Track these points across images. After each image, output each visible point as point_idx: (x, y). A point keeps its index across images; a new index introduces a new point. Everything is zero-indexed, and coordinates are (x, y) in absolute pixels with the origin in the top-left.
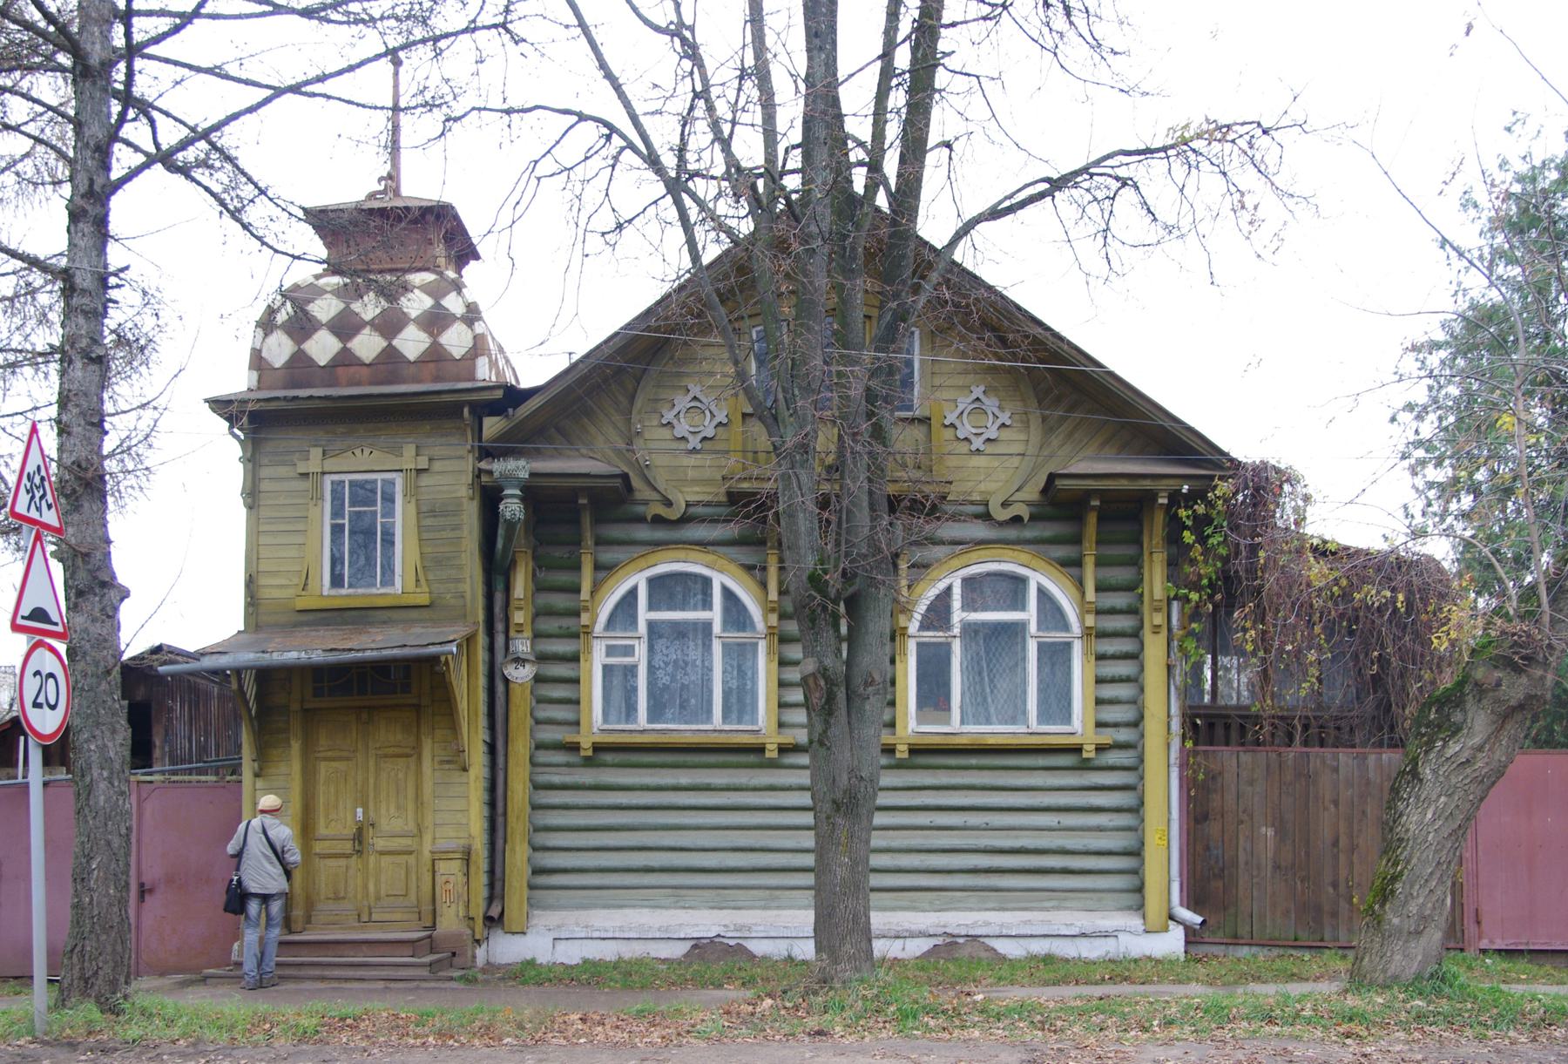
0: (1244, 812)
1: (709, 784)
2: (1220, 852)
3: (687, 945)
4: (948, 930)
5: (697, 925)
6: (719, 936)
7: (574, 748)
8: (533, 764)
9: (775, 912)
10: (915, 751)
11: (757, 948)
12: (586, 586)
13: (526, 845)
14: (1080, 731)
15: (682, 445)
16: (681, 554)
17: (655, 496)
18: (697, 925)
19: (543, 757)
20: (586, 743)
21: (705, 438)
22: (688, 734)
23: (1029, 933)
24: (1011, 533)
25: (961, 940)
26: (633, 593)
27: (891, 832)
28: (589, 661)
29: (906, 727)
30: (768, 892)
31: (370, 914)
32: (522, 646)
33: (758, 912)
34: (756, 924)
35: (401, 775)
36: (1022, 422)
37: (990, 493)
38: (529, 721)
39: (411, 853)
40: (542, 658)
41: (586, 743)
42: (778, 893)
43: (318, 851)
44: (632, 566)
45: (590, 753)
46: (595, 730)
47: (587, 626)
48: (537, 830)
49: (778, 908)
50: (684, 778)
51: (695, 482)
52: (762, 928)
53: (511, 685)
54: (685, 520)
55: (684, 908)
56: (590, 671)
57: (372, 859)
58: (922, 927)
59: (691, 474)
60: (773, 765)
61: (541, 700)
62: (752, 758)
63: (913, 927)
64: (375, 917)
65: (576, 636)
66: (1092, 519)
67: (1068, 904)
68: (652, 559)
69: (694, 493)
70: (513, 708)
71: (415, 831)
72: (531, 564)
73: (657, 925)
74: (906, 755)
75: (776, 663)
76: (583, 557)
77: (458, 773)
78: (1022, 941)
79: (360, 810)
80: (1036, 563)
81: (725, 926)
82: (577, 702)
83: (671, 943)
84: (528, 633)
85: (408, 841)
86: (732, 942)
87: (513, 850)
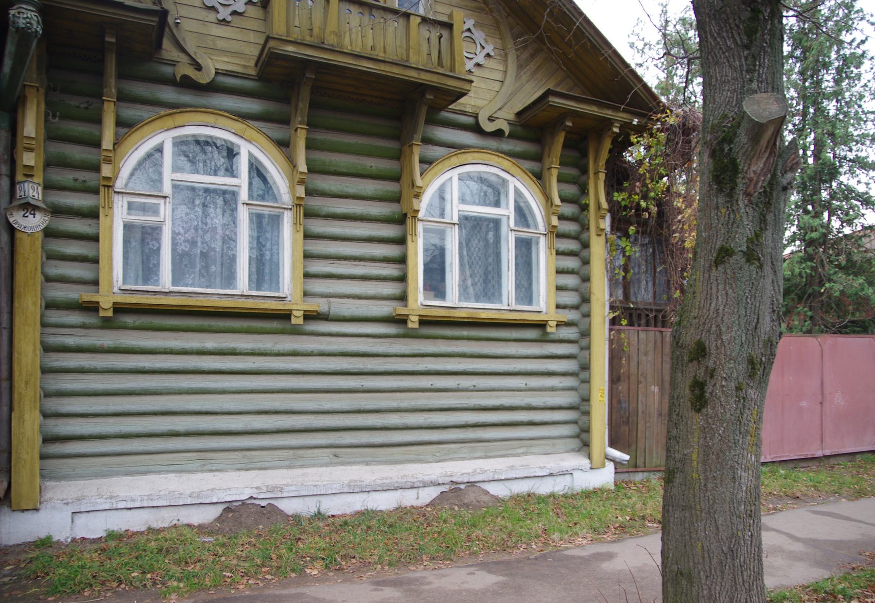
0: (641, 375)
1: (234, 349)
2: (627, 404)
3: (220, 509)
4: (454, 479)
5: (229, 489)
6: (251, 498)
7: (92, 308)
8: (44, 325)
9: (300, 471)
10: (424, 322)
11: (289, 507)
12: (107, 142)
13: (37, 413)
14: (544, 310)
15: (211, 16)
16: (211, 119)
17: (183, 58)
18: (229, 489)
19: (56, 316)
20: (106, 302)
21: (234, 13)
22: (215, 298)
23: (514, 476)
24: (492, 143)
25: (462, 487)
26: (159, 149)
27: (398, 394)
28: (110, 215)
29: (416, 300)
30: (291, 452)
32: (32, 191)
33: (284, 472)
34: (287, 485)
36: (500, 55)
37: (480, 108)
38: (40, 278)
40: (57, 211)
41: (106, 302)
42: (301, 452)
44: (157, 123)
45: (110, 314)
46: (116, 290)
47: (108, 179)
48: (48, 395)
49: (302, 466)
50: (210, 342)
51: (223, 52)
52: (293, 488)
53: (18, 235)
54: (212, 88)
55: (211, 471)
56: (111, 228)
58: (433, 478)
59: (220, 44)
60: (297, 331)
61: (52, 256)
62: (275, 325)
63: (427, 478)
65: (96, 192)
66: (561, 138)
67: (533, 450)
68: (180, 119)
69: (224, 63)
70: (20, 260)
72: (43, 106)
73: (188, 492)
74: (416, 326)
75: (301, 235)
76: (106, 104)
78: (506, 483)
80: (515, 170)
81: (257, 488)
82: (96, 261)
83: (202, 508)
84: (39, 179)
86: (264, 503)
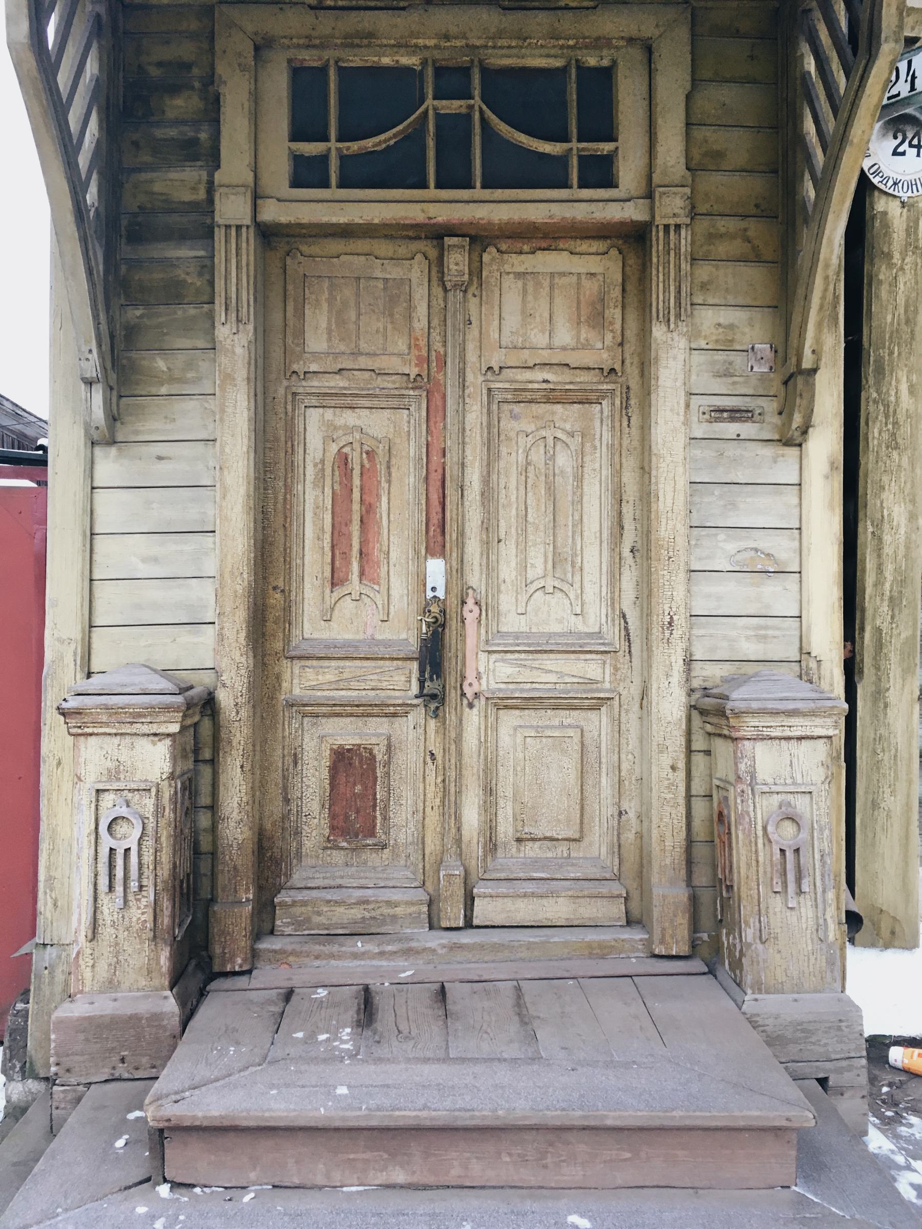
31: (470, 900)
35: (564, 460)
39: (597, 704)
43: (297, 691)
57: (473, 719)
64: (483, 911)
71: (613, 634)
77: (767, 451)
79: (436, 569)
85: (592, 669)
87: (879, 694)
